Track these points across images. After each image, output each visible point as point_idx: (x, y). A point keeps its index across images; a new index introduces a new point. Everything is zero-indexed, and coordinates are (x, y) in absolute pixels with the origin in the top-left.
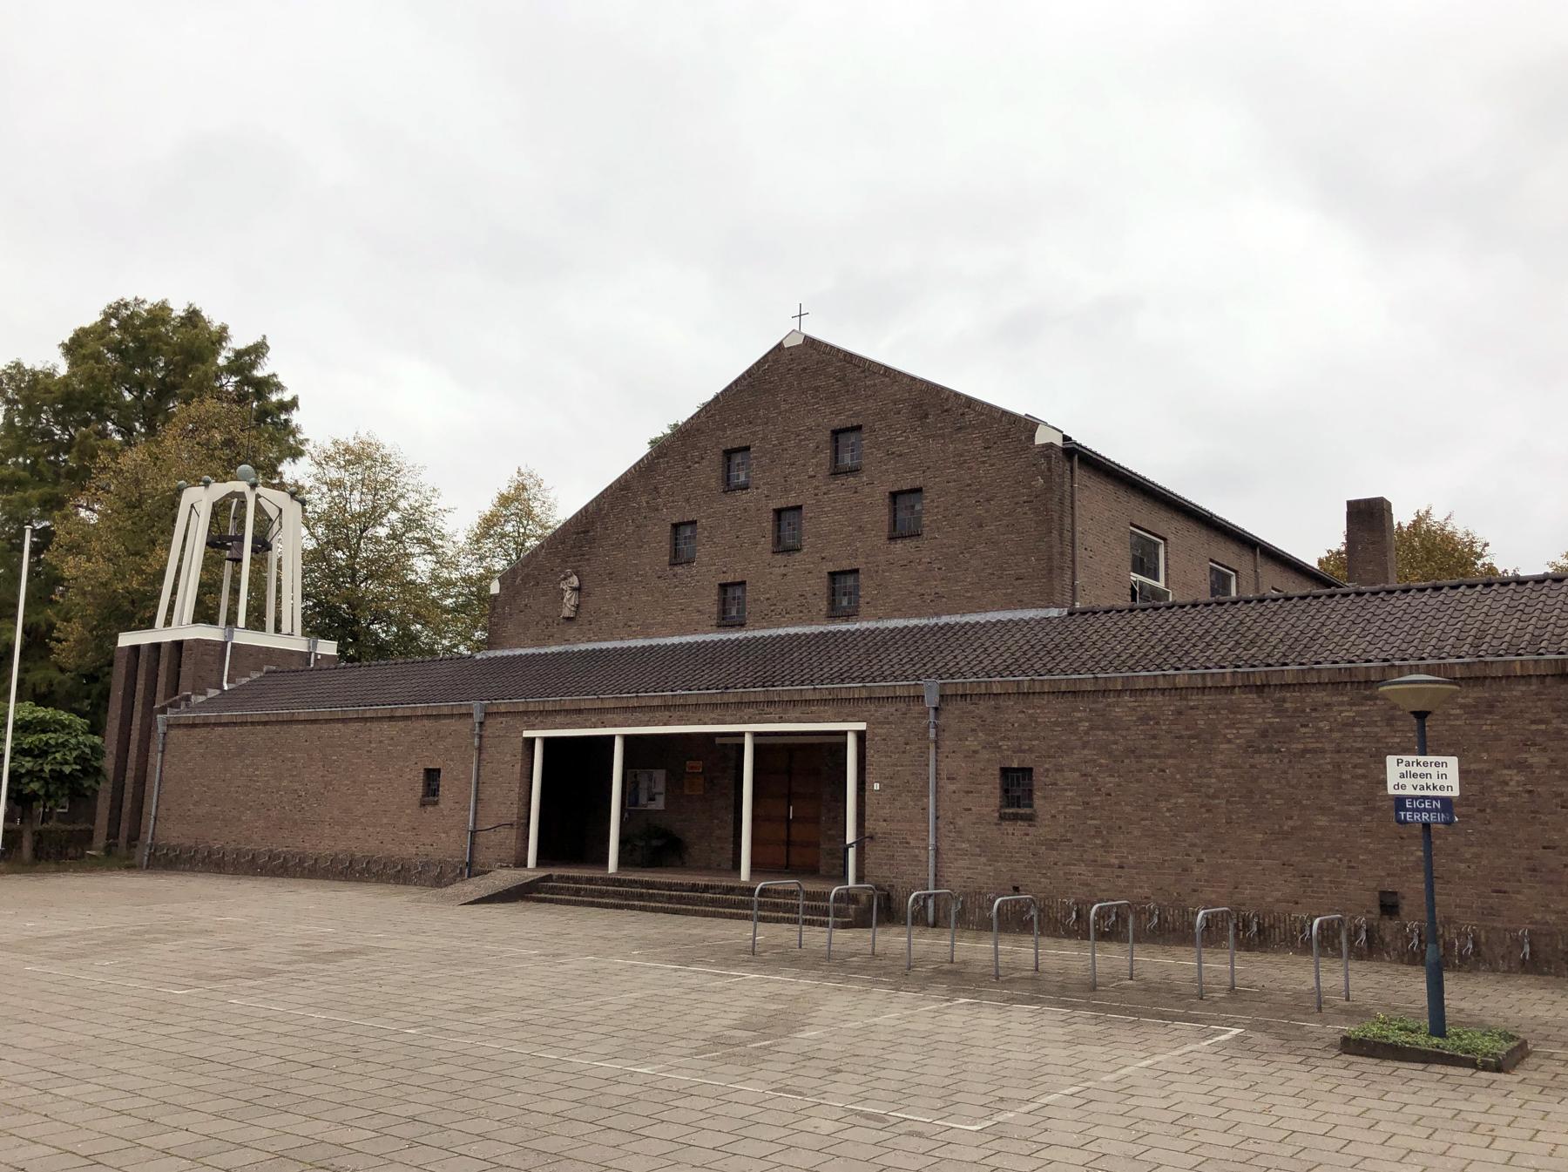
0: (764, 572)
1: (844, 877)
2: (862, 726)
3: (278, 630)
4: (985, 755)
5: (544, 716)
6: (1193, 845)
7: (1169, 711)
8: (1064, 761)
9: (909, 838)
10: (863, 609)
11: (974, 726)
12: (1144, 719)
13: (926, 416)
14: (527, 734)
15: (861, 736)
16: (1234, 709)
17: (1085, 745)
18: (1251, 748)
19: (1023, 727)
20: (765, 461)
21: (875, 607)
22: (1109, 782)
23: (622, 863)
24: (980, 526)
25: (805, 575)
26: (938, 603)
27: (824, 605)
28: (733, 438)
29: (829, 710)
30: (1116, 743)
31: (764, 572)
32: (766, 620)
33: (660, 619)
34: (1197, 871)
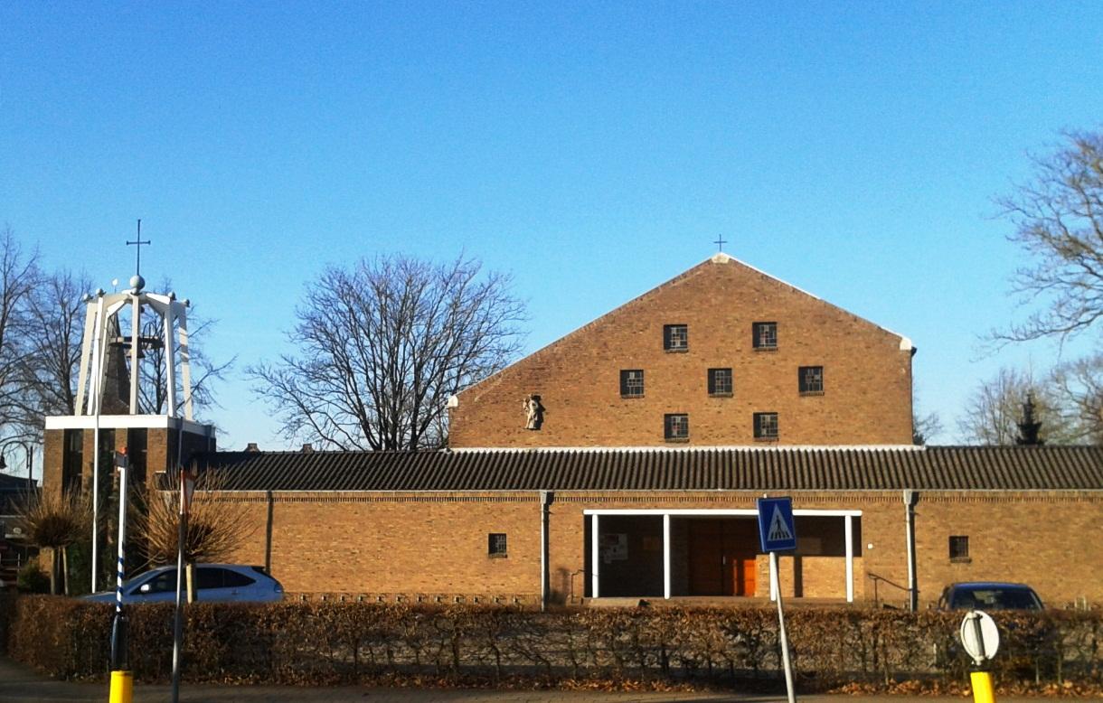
0: (702, 409)
1: (662, 594)
2: (858, 513)
3: (84, 412)
4: (941, 529)
5: (603, 502)
6: (1058, 573)
7: (1045, 509)
8: (988, 532)
9: (893, 573)
10: (781, 437)
11: (932, 514)
12: (1032, 512)
13: (824, 323)
14: (587, 512)
15: (856, 521)
16: (1079, 508)
17: (999, 525)
18: (1087, 527)
19: (964, 515)
20: (700, 336)
21: (790, 436)
22: (1013, 543)
23: (673, 593)
24: (864, 393)
25: (737, 410)
26: (835, 437)
27: (751, 433)
28: (674, 317)
29: (835, 504)
30: (1017, 524)
31: (702, 409)
32: (705, 439)
33: (613, 434)
34: (1059, 585)
